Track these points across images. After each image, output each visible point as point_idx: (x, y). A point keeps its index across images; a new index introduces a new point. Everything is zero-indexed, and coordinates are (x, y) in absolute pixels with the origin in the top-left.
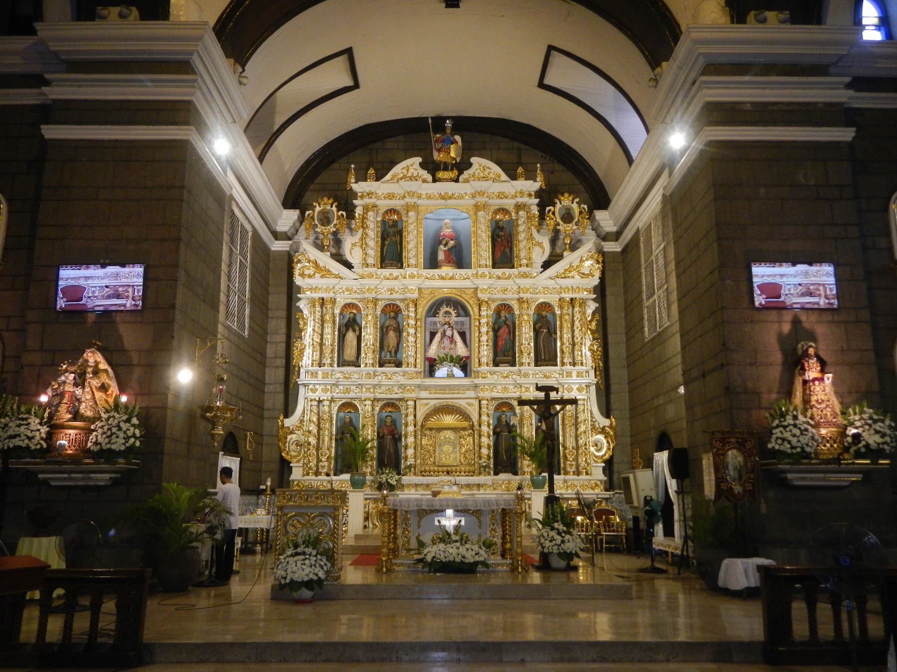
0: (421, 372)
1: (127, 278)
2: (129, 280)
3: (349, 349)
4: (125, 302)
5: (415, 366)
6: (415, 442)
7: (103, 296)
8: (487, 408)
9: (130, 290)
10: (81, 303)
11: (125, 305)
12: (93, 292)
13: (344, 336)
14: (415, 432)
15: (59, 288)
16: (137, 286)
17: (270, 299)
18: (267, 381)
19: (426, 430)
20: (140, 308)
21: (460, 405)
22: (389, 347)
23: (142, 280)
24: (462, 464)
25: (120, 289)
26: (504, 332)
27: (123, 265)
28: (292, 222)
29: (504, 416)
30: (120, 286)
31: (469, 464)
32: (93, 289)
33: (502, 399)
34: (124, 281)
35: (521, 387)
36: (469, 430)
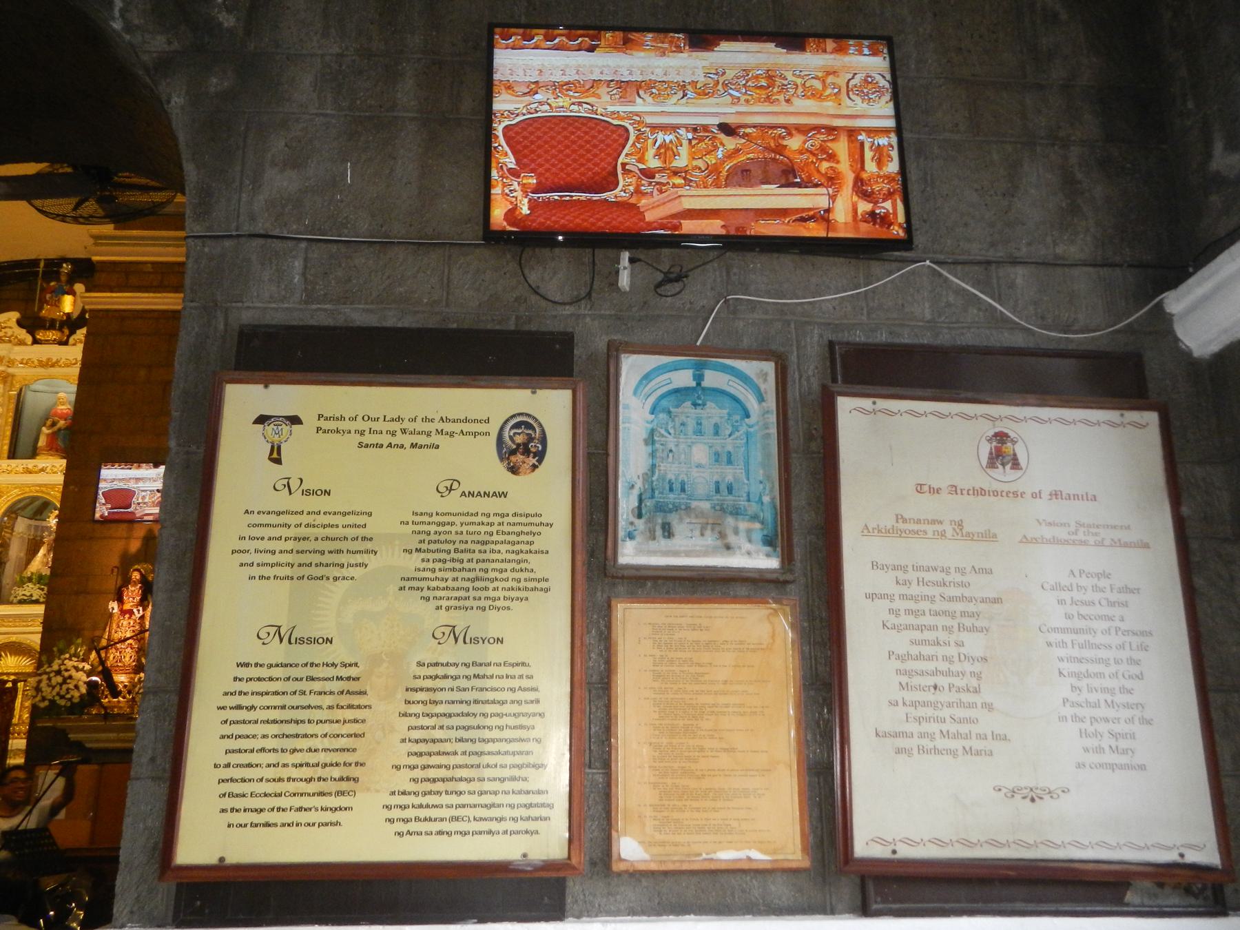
1: (817, 95)
2: (829, 106)
4: (823, 202)
7: (714, 170)
9: (841, 147)
10: (609, 196)
11: (824, 216)
12: (665, 152)
15: (499, 129)
16: (871, 132)
20: (897, 232)
23: (889, 109)
25: (794, 143)
27: (793, 41)
30: (790, 130)
32: (661, 137)
34: (803, 109)
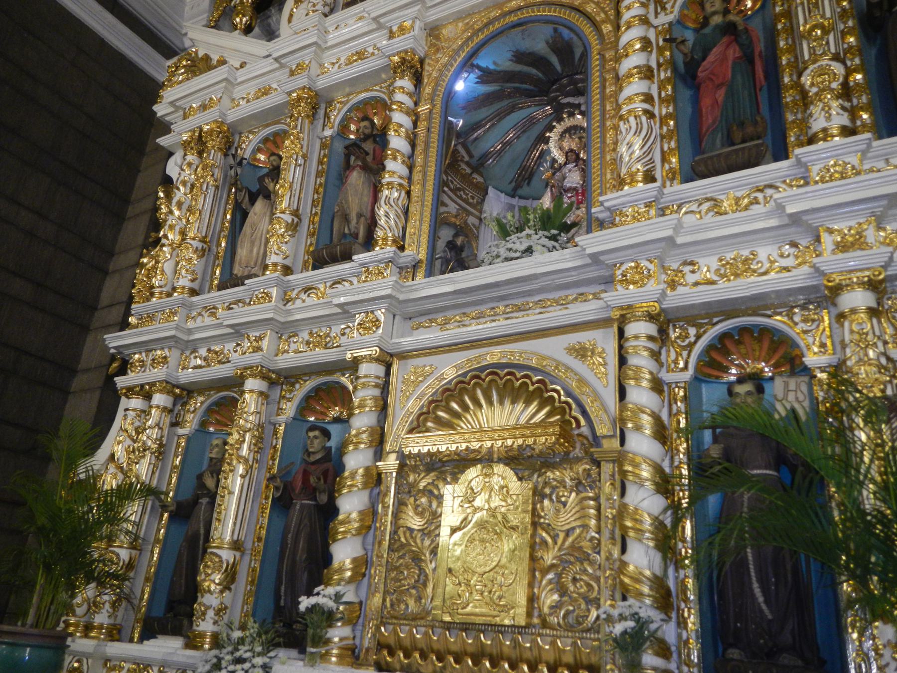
0: (415, 266)
3: (247, 245)
5: (402, 248)
6: (370, 515)
8: (655, 355)
13: (245, 215)
14: (375, 479)
17: (139, 181)
18: (82, 365)
19: (414, 469)
21: (544, 358)
22: (346, 219)
24: (545, 624)
26: (724, 58)
28: (206, 15)
29: (741, 389)
31: (575, 626)
33: (727, 309)
35: (818, 239)
36: (578, 460)
